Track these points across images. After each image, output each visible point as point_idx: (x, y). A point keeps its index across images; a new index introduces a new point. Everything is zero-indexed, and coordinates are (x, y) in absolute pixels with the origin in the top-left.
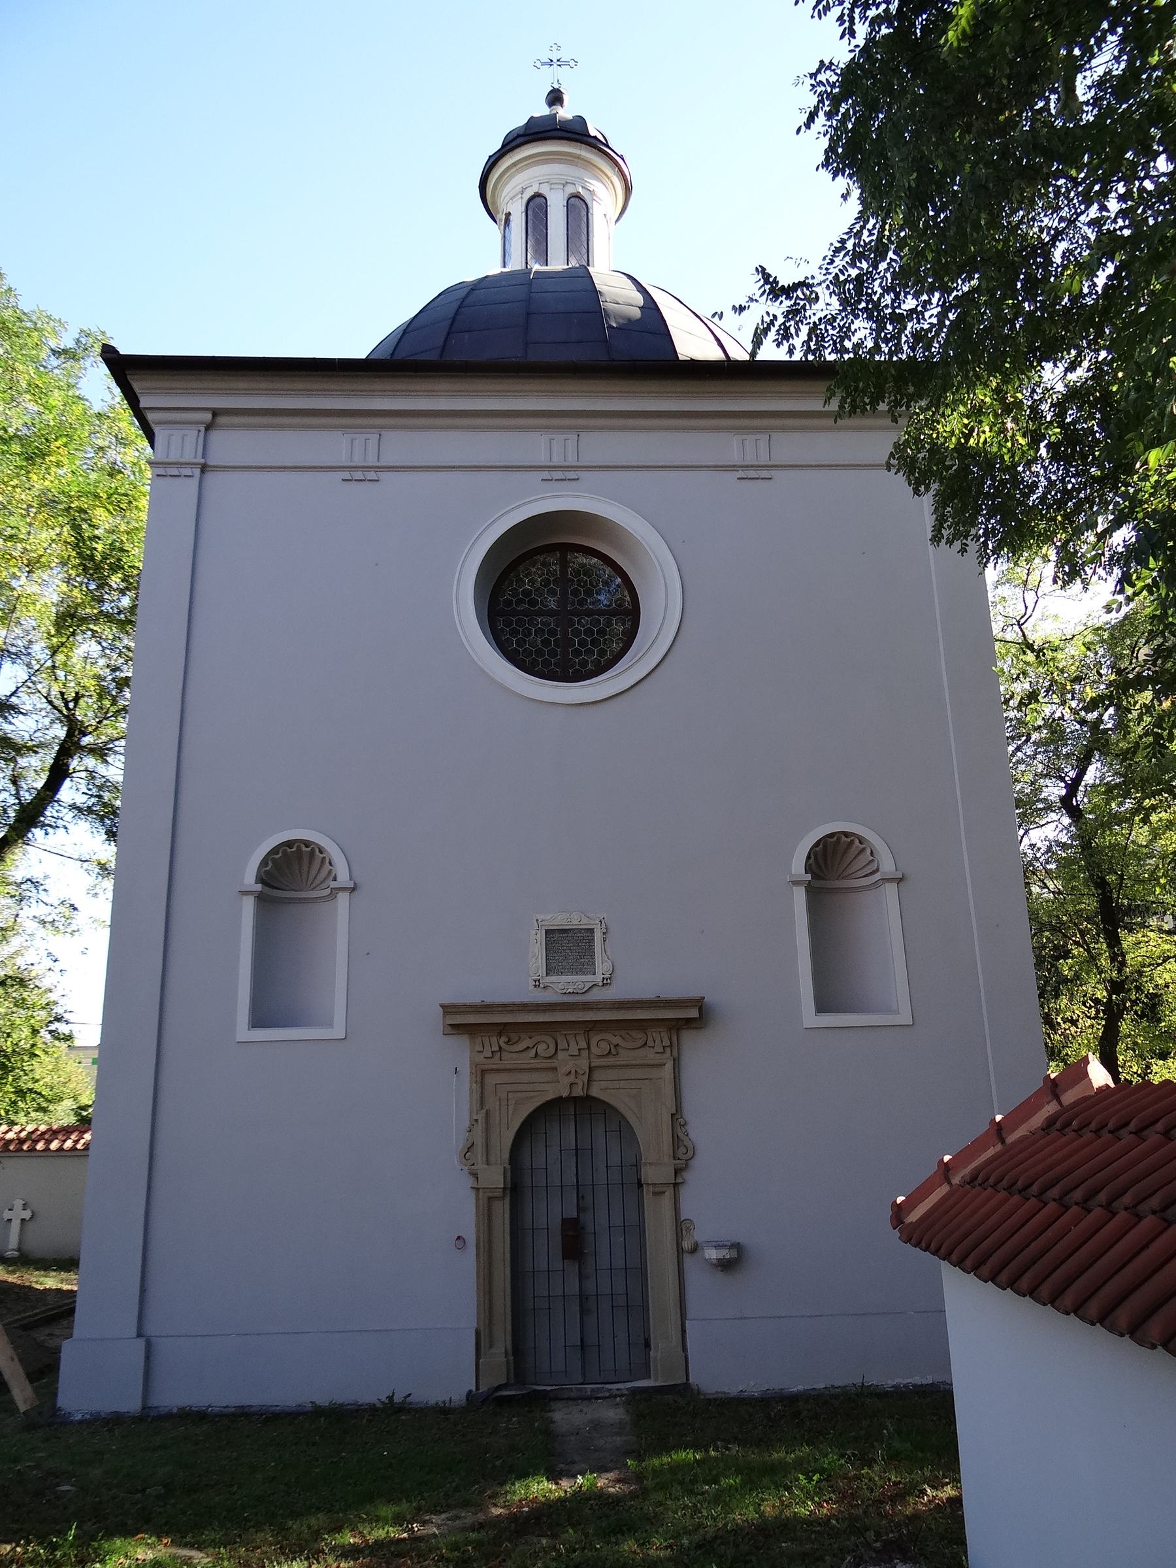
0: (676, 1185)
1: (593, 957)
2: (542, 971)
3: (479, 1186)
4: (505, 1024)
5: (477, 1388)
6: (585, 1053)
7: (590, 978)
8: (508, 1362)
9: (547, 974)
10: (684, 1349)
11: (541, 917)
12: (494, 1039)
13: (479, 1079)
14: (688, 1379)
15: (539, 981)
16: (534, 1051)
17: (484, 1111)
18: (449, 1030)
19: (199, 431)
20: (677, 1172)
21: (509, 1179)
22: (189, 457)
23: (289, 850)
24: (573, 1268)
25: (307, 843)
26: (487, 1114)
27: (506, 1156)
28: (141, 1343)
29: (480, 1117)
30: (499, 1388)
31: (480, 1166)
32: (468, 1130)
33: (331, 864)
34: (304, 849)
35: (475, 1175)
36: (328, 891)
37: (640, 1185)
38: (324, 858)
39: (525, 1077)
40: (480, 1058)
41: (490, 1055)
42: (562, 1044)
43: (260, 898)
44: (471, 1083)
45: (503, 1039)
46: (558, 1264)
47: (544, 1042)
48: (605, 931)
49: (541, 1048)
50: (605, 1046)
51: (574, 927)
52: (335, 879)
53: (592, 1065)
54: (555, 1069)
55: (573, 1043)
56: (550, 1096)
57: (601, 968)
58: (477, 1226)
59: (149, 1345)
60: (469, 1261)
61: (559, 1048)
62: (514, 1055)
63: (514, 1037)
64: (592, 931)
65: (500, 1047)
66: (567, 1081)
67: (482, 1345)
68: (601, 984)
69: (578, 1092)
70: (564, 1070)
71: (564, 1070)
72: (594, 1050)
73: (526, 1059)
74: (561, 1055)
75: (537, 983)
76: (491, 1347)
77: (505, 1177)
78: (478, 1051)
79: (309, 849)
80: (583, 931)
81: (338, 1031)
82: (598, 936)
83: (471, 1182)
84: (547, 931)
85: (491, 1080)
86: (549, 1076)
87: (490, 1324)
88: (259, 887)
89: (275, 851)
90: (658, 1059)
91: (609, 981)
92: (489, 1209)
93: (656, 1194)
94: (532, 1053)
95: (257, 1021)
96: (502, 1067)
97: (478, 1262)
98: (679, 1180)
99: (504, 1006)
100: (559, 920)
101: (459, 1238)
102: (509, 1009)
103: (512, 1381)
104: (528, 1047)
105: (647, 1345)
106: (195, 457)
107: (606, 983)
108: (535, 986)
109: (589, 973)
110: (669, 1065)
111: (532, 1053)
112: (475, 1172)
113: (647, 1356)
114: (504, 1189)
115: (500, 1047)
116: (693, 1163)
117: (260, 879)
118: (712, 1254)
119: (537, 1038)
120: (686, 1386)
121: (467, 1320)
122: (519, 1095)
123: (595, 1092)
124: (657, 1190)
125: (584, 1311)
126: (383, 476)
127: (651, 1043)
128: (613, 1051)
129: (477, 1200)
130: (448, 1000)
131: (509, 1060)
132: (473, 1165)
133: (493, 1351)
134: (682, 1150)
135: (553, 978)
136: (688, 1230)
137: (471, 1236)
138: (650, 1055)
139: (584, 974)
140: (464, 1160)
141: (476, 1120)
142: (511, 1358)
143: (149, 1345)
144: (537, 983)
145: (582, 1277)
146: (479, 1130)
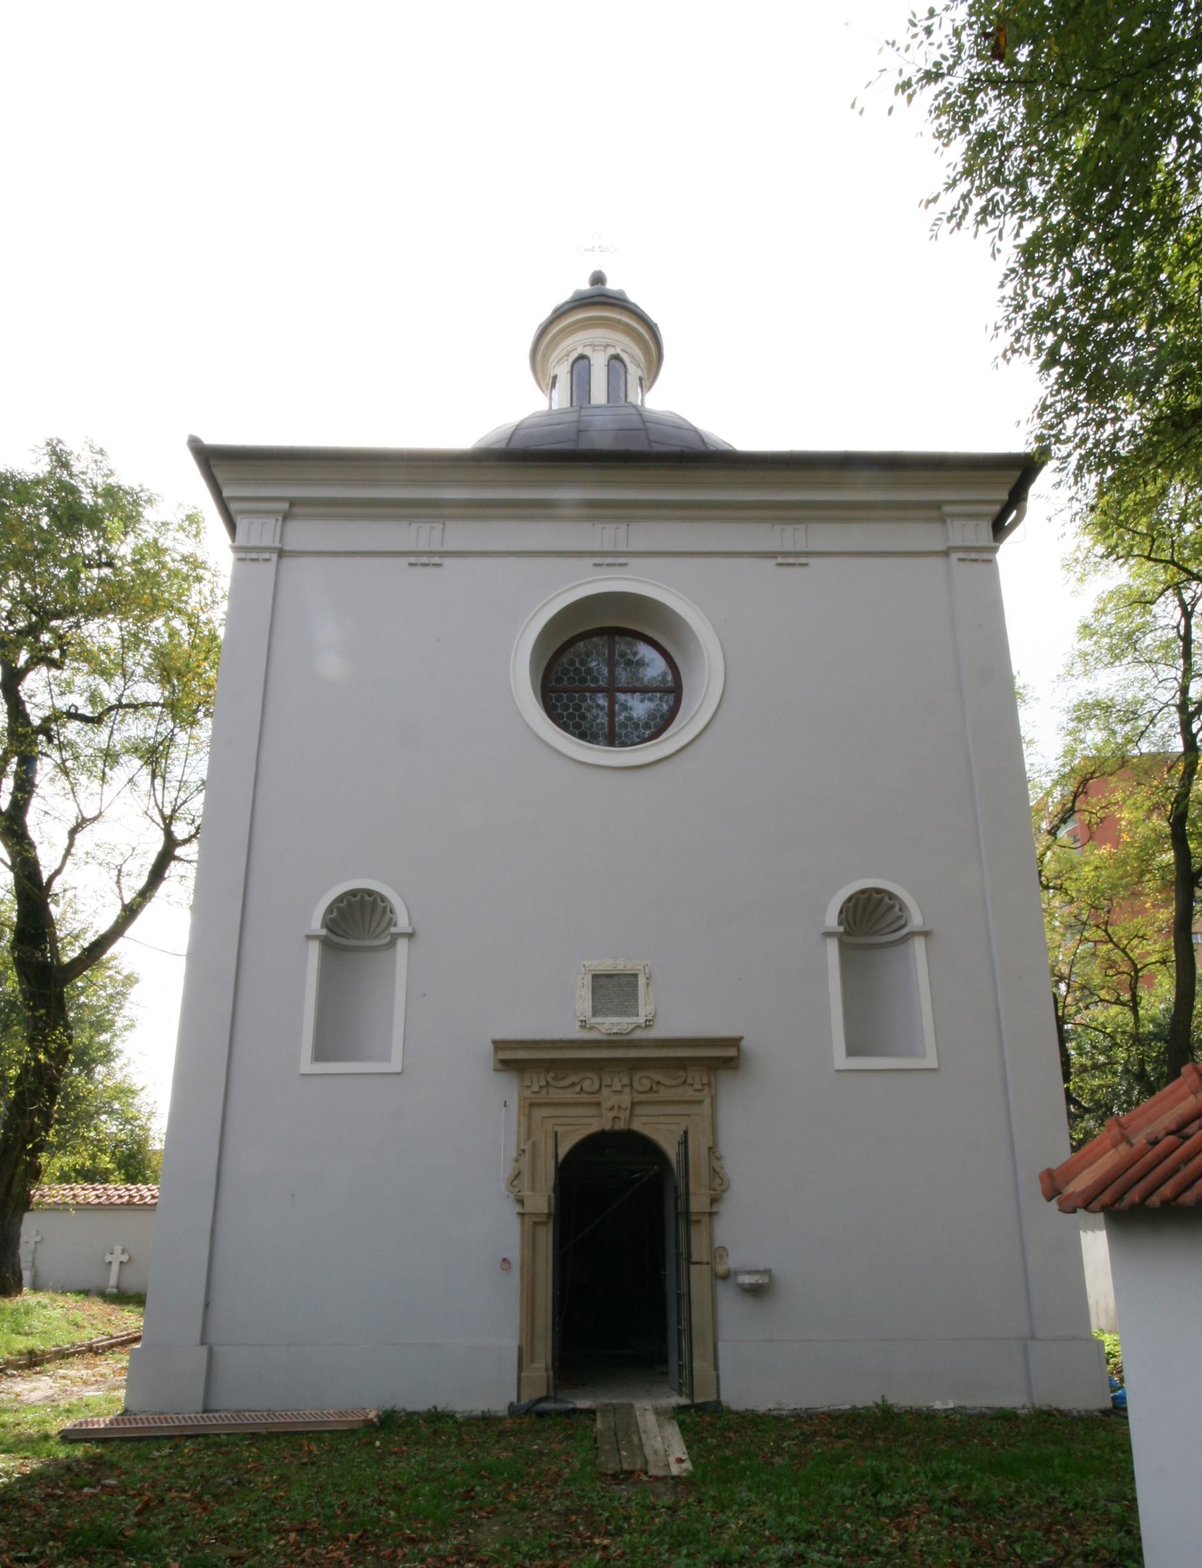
0: (711, 1214)
1: (636, 1000)
2: (589, 1012)
4: (553, 1061)
5: (519, 1400)
6: (627, 1090)
7: (633, 1020)
8: (548, 1377)
9: (594, 1015)
10: (716, 1368)
11: (587, 963)
13: (527, 1112)
14: (718, 1396)
17: (531, 1142)
18: (499, 1066)
19: (277, 520)
22: (268, 542)
25: (370, 893)
26: (534, 1145)
28: (204, 1349)
29: (527, 1147)
30: (540, 1400)
31: (526, 1193)
33: (391, 912)
34: (367, 898)
35: (521, 1201)
36: (388, 939)
38: (385, 908)
39: (571, 1111)
40: (528, 1093)
42: (607, 1081)
43: (326, 943)
45: (552, 1075)
47: (588, 1078)
49: (586, 1084)
50: (647, 1084)
52: (395, 925)
53: (635, 1100)
54: (598, 1104)
55: (616, 1080)
57: (645, 1009)
58: (522, 1249)
59: (211, 1352)
60: (513, 1282)
61: (604, 1083)
64: (635, 976)
65: (547, 1082)
67: (525, 1359)
68: (643, 1025)
71: (608, 1104)
72: (637, 1086)
73: (569, 1095)
74: (605, 1091)
75: (583, 1025)
76: (532, 1361)
77: (549, 1205)
79: (371, 899)
81: (395, 1065)
82: (642, 980)
83: (518, 1209)
84: (595, 977)
85: (539, 1113)
86: (592, 1111)
87: (532, 1342)
88: (324, 932)
89: (340, 899)
92: (534, 1234)
94: (578, 1088)
95: (319, 1055)
97: (522, 1284)
98: (714, 1209)
100: (605, 965)
101: (504, 1260)
103: (552, 1394)
104: (574, 1084)
106: (273, 542)
107: (648, 1025)
108: (581, 1027)
110: (707, 1101)
111: (578, 1088)
114: (549, 1215)
116: (727, 1195)
117: (325, 925)
118: (747, 1280)
120: (718, 1403)
121: (510, 1341)
123: (637, 1126)
126: (447, 561)
127: (690, 1081)
128: (655, 1088)
129: (523, 1224)
130: (500, 1036)
131: (555, 1095)
133: (535, 1365)
134: (718, 1181)
135: (598, 1020)
136: (721, 1257)
137: (515, 1256)
138: (690, 1094)
140: (511, 1188)
141: (524, 1151)
142: (551, 1373)
143: (211, 1352)
146: (526, 1160)
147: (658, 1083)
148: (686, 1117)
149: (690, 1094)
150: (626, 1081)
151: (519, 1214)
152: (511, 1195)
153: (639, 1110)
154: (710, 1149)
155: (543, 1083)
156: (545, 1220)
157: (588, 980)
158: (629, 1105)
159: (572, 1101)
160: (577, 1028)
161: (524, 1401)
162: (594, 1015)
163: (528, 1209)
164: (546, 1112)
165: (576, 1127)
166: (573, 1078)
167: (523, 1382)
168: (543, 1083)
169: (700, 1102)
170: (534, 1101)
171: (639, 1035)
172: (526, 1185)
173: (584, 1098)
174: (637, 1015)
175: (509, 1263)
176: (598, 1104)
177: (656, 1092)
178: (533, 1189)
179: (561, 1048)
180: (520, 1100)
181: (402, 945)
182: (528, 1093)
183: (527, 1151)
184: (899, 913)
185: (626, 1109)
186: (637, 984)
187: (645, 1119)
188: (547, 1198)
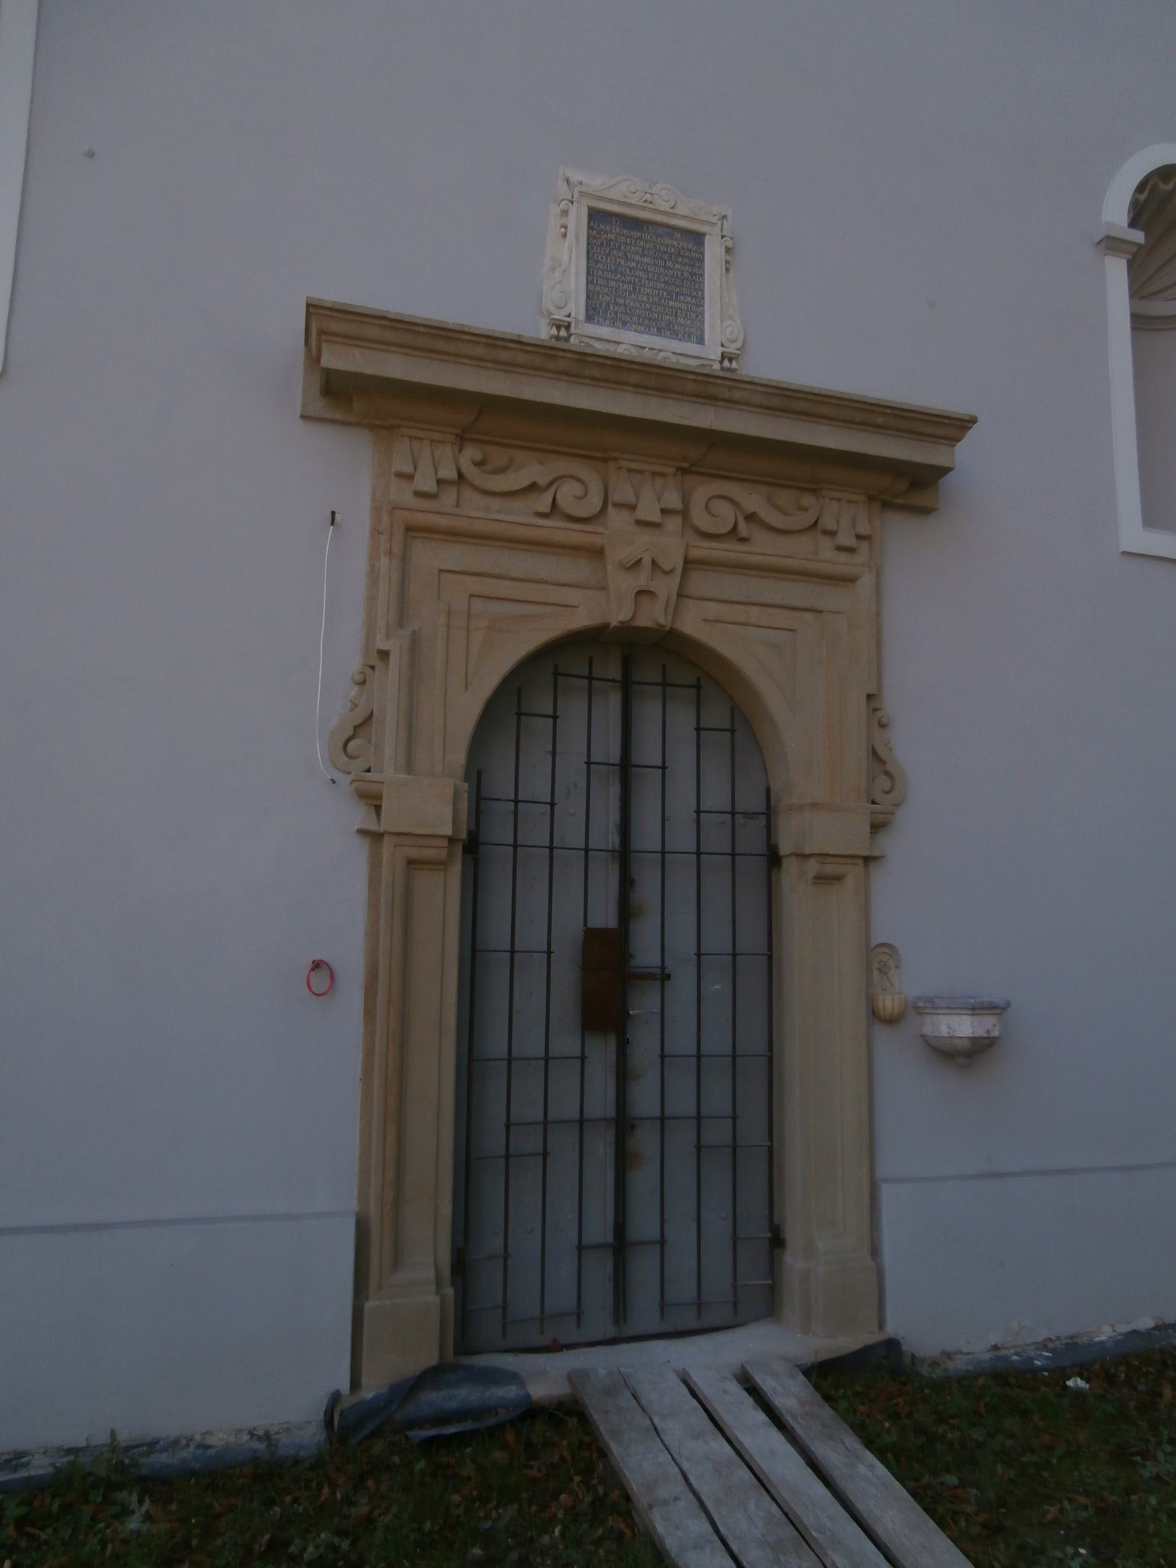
0: (868, 860)
1: (699, 302)
2: (577, 308)
3: (382, 829)
9: (589, 318)
10: (875, 1251)
11: (575, 177)
12: (448, 451)
13: (397, 549)
15: (568, 327)
16: (547, 497)
18: (319, 406)
20: (877, 827)
21: (464, 817)
24: (602, 1052)
26: (415, 640)
27: (459, 757)
29: (396, 646)
31: (389, 773)
32: (358, 678)
35: (373, 800)
37: (774, 859)
40: (403, 494)
41: (430, 486)
44: (373, 558)
45: (471, 453)
46: (567, 1042)
47: (579, 480)
48: (730, 244)
49: (567, 493)
50: (726, 515)
51: (659, 218)
53: (695, 553)
54: (597, 553)
56: (581, 620)
58: (372, 934)
61: (616, 497)
62: (496, 503)
63: (498, 457)
64: (698, 238)
65: (460, 475)
66: (624, 584)
69: (653, 616)
70: (619, 554)
74: (617, 519)
76: (396, 1264)
77: (455, 812)
78: (400, 475)
80: (678, 235)
82: (713, 252)
83: (361, 817)
84: (595, 215)
87: (398, 1202)
90: (841, 564)
91: (734, 365)
93: (822, 879)
94: (544, 504)
96: (461, 524)
99: (492, 341)
101: (317, 965)
102: (504, 356)
104: (533, 487)
105: (777, 1241)
109: (687, 337)
113: (773, 1268)
114: (451, 840)
115: (460, 475)
119: (562, 466)
122: (497, 608)
123: (692, 624)
124: (830, 869)
125: (623, 1161)
129: (375, 865)
130: (333, 294)
132: (369, 770)
139: (675, 335)
140: (346, 759)
141: (384, 655)
142: (450, 1291)
144: (563, 333)
145: (623, 1075)
146: (391, 679)
147: (751, 517)
148: (809, 616)
149: (826, 557)
150: (673, 500)
151: (362, 832)
152: (344, 780)
153: (700, 583)
154: (870, 697)
155: (449, 473)
156: (443, 854)
157: (578, 220)
158: (681, 563)
159: (519, 532)
162: (589, 318)
163: (394, 818)
164: (454, 556)
165: (534, 609)
166: (532, 471)
168: (449, 473)
169: (850, 580)
170: (420, 519)
172: (388, 751)
173: (557, 530)
174: (701, 341)
175: (332, 976)
176: (597, 553)
177: (743, 540)
178: (409, 766)
180: (376, 511)
182: (403, 494)
183: (394, 659)
185: (672, 571)
186: (702, 261)
187: (712, 609)
188: (449, 793)
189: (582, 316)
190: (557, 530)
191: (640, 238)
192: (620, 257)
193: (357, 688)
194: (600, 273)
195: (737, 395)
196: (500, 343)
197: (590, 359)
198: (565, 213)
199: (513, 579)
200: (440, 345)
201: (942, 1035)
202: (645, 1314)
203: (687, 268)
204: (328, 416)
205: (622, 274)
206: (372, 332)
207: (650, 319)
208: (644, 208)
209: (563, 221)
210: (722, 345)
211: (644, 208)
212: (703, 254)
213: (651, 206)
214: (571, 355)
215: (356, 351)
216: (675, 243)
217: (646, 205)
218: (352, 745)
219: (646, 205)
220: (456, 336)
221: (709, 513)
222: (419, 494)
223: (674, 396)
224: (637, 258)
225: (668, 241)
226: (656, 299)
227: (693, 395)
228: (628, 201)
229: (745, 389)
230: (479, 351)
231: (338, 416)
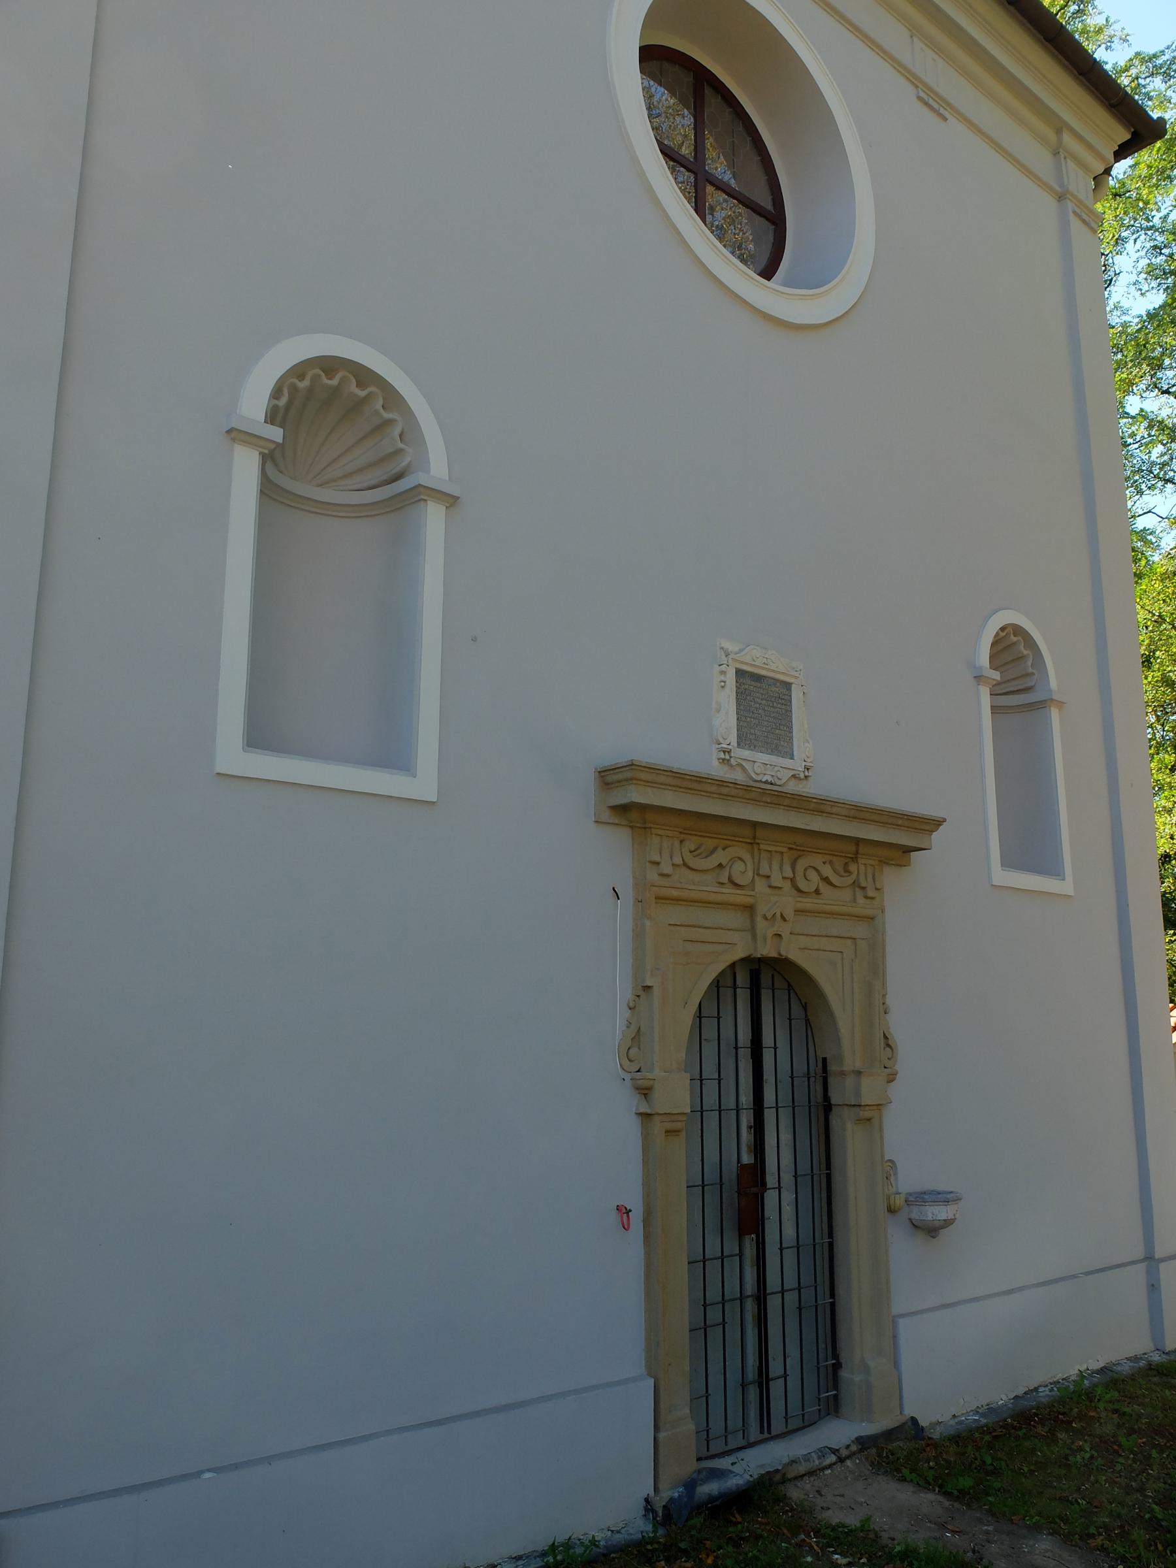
2: (733, 739)
7: (787, 762)
15: (729, 752)
18: (606, 815)
23: (326, 381)
35: (645, 1092)
45: (690, 844)
64: (788, 686)
68: (802, 776)
84: (740, 673)
102: (725, 791)
112: (646, 1083)
135: (746, 754)
141: (647, 988)
148: (849, 942)
159: (712, 897)
160: (715, 763)
161: (670, 1492)
164: (676, 914)
167: (662, 1450)
170: (663, 892)
171: (793, 787)
173: (730, 894)
179: (725, 797)
181: (434, 515)
182: (652, 875)
184: (1030, 670)
189: (735, 744)
190: (730, 894)
191: (760, 687)
192: (751, 701)
193: (630, 1011)
194: (742, 712)
195: (834, 810)
196: (725, 784)
197: (768, 792)
198: (723, 673)
199: (705, 928)
200: (695, 786)
201: (929, 1219)
202: (777, 1425)
203: (783, 707)
204: (611, 822)
205: (753, 713)
206: (662, 779)
207: (767, 743)
208: (763, 668)
209: (722, 678)
210: (805, 761)
211: (763, 668)
212: (790, 696)
213: (767, 666)
214: (759, 790)
215: (649, 790)
216: (777, 690)
217: (764, 666)
218: (631, 1051)
219: (764, 666)
220: (704, 780)
221: (807, 880)
222: (662, 875)
223: (803, 811)
224: (759, 701)
225: (773, 689)
226: (770, 729)
227: (813, 811)
228: (754, 663)
229: (839, 807)
230: (714, 788)
231: (617, 822)
